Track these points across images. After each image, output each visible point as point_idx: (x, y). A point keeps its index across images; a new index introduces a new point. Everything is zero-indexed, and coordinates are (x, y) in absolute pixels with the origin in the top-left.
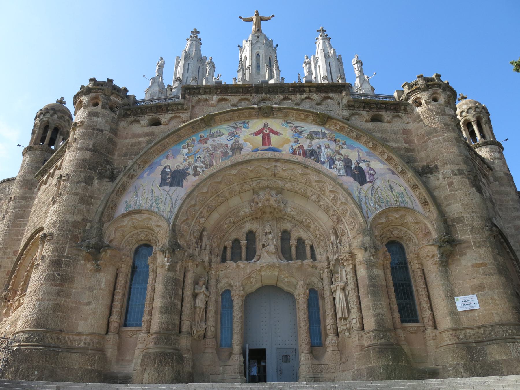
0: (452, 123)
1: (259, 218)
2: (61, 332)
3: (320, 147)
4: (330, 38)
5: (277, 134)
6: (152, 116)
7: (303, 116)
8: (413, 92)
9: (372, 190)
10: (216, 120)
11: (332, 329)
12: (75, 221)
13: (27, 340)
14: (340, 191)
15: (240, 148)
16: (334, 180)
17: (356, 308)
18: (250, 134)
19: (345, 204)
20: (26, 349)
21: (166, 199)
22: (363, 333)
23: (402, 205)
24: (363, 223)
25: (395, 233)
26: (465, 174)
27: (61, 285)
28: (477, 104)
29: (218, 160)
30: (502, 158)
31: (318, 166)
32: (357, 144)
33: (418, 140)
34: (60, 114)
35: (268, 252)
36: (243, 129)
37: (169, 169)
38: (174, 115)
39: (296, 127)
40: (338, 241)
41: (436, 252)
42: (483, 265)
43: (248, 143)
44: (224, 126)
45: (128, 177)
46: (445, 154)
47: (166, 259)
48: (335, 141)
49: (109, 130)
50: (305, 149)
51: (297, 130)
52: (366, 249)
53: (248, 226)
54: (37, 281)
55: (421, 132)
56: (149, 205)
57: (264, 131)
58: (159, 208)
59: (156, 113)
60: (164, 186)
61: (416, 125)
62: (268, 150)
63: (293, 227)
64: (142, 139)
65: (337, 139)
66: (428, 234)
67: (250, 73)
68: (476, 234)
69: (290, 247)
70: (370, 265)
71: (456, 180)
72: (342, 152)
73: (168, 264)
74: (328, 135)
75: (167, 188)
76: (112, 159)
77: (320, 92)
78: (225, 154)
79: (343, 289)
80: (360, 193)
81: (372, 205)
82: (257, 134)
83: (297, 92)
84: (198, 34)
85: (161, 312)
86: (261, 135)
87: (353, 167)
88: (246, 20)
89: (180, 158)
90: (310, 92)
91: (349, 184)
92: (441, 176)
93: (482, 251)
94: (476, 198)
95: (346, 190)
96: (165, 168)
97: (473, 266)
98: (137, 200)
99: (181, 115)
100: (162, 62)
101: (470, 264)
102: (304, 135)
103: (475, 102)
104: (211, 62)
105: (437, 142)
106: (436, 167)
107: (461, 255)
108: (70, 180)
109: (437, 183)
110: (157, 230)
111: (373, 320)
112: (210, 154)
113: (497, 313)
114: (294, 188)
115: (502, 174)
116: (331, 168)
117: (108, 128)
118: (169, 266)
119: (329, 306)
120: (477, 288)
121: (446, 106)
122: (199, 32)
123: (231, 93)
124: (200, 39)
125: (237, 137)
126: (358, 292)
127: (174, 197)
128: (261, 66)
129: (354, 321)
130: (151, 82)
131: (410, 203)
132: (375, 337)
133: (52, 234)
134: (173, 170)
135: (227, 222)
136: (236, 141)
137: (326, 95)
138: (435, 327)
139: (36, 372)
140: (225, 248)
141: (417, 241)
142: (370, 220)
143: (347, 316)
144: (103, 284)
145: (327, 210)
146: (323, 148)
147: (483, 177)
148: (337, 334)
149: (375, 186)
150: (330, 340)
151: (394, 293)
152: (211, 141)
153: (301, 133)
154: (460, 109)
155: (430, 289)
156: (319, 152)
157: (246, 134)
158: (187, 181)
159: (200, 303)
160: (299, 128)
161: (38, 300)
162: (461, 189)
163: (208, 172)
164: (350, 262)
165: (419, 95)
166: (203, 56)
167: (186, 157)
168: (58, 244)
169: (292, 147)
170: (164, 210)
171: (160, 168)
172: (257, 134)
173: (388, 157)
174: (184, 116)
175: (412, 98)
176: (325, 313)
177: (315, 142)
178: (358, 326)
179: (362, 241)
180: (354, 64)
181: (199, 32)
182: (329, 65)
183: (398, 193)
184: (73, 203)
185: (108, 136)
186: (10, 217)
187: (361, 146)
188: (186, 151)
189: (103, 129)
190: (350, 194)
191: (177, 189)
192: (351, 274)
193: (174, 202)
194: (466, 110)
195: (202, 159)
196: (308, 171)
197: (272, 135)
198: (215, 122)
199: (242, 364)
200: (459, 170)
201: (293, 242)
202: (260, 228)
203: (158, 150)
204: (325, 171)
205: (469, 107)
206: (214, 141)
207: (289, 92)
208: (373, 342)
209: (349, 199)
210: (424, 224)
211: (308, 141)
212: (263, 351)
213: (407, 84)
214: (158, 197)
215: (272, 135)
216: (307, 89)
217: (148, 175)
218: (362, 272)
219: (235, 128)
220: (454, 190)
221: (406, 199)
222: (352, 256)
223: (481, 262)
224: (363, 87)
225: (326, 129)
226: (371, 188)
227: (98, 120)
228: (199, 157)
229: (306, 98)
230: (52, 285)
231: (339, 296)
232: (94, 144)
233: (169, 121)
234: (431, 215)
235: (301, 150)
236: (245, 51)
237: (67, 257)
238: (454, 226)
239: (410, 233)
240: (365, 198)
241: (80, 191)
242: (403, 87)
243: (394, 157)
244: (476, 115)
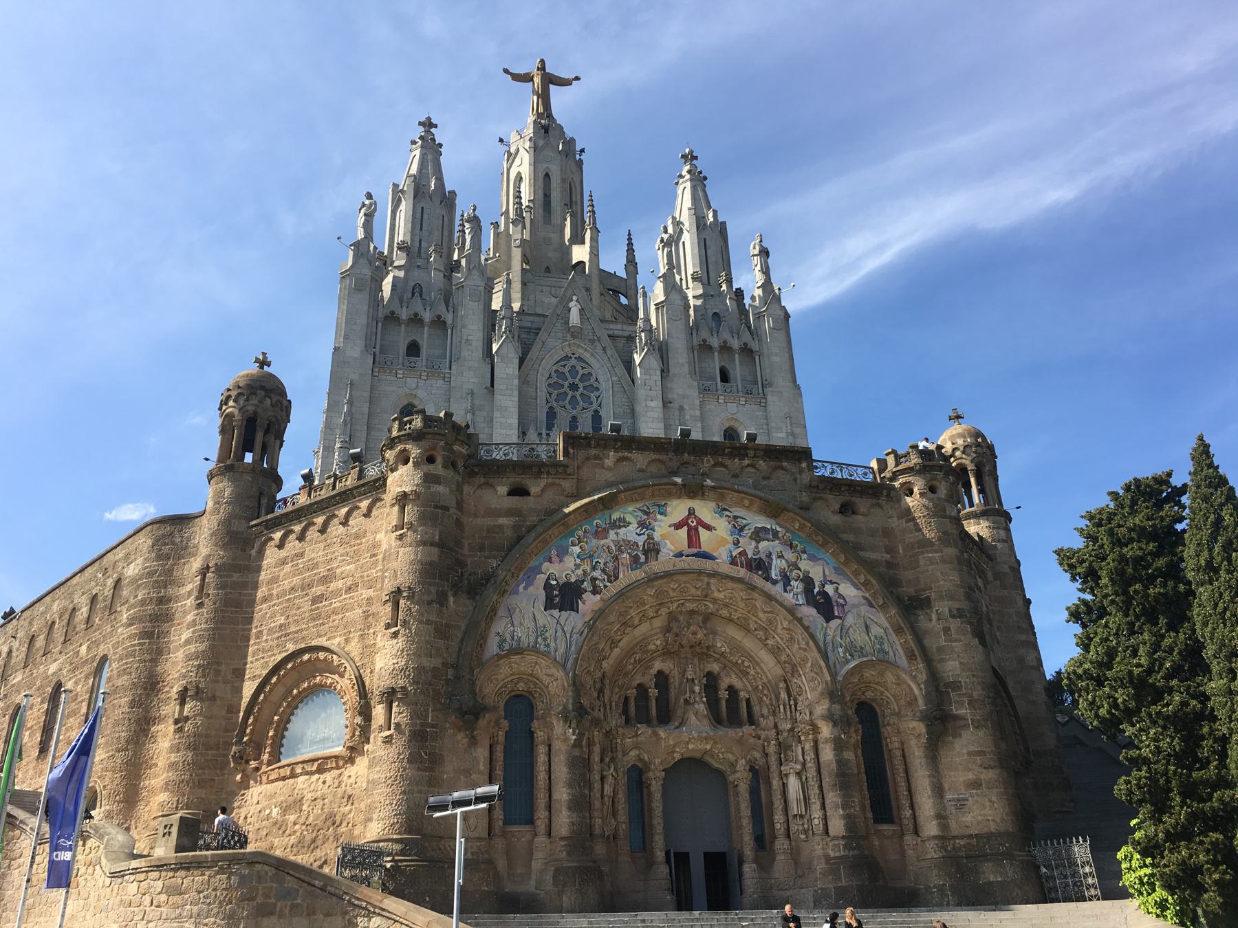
0: (954, 531)
1: (673, 653)
2: (442, 838)
3: (769, 555)
4: (705, 178)
5: (708, 528)
6: (514, 479)
7: (747, 503)
8: (903, 472)
10: (619, 499)
11: (783, 829)
12: (434, 668)
13: (402, 853)
14: (800, 630)
15: (658, 551)
16: (791, 611)
17: (818, 803)
18: (670, 526)
19: (805, 650)
20: (407, 866)
21: (556, 632)
22: (828, 840)
23: (881, 656)
24: (829, 683)
25: (869, 694)
26: (966, 616)
27: (432, 769)
28: (979, 440)
29: (626, 568)
30: (1008, 540)
31: (768, 586)
32: (821, 554)
33: (903, 549)
34: (275, 398)
35: (696, 714)
36: (659, 517)
37: (556, 580)
38: (550, 480)
39: (735, 517)
40: (792, 702)
41: (924, 730)
42: (979, 753)
44: (631, 509)
45: (499, 593)
46: (942, 582)
47: (571, 730)
48: (791, 546)
49: (455, 506)
51: (737, 522)
52: (835, 724)
53: (658, 665)
54: (395, 762)
55: (910, 538)
56: (532, 640)
57: (690, 522)
58: (547, 646)
59: (521, 474)
60: (551, 609)
61: (903, 523)
62: (697, 555)
63: (724, 668)
64: (503, 521)
65: (795, 543)
66: (912, 702)
67: (531, 219)
68: (975, 709)
69: (718, 700)
70: (839, 746)
71: (955, 624)
73: (574, 737)
74: (780, 535)
75: (556, 612)
76: (462, 555)
77: (769, 457)
78: (635, 559)
79: (799, 774)
80: (825, 635)
81: (842, 654)
82: (678, 526)
83: (735, 455)
84: (433, 130)
85: (570, 808)
86: (685, 528)
87: (816, 590)
88: (517, 77)
89: (570, 562)
90: (755, 456)
91: (811, 619)
92: (934, 616)
93: (981, 734)
94: (978, 655)
95: (806, 629)
96: (548, 578)
97: (969, 754)
98: (514, 631)
99: (563, 483)
100: (371, 205)
101: (965, 751)
102: (748, 532)
103: (977, 433)
104: (475, 216)
105: (931, 561)
106: (928, 600)
107: (954, 737)
108: (416, 597)
109: (929, 625)
110: (546, 680)
111: (842, 822)
112: (613, 557)
113: (993, 820)
114: (731, 615)
115: (1006, 569)
116: (785, 591)
117: (454, 504)
118: (575, 740)
119: (777, 797)
120: (971, 784)
121: (947, 501)
122: (436, 126)
123: (638, 449)
124: (440, 145)
125: (651, 529)
126: (821, 782)
127: (568, 629)
128: (552, 205)
129: (816, 821)
130: (351, 253)
131: (891, 653)
132: (845, 847)
133: (404, 688)
134: (561, 582)
135: (632, 661)
136: (650, 537)
137: (778, 463)
138: (916, 832)
139: (428, 899)
140: (627, 699)
141: (896, 708)
142: (840, 678)
143: (804, 813)
144: (481, 764)
145: (775, 651)
146: (774, 557)
147: (980, 577)
148: (788, 836)
149: (846, 624)
150: (781, 844)
151: (866, 784)
152: (612, 533)
153: (742, 529)
154: (953, 444)
155: (913, 781)
156: (768, 563)
157: (663, 524)
158: (584, 603)
159: (608, 790)
160: (739, 520)
161: (403, 793)
162: (960, 640)
163: (613, 588)
164: (811, 737)
165: (911, 478)
166: (447, 189)
167: (578, 561)
168: (416, 704)
169: (731, 552)
170: (556, 650)
171: (541, 579)
172: (678, 526)
173: (866, 580)
174: (568, 485)
175: (901, 480)
176: (771, 803)
177: (763, 545)
178: (821, 829)
179: (829, 710)
180: (754, 255)
181: (436, 126)
182: (703, 245)
183: (876, 636)
184: (427, 638)
185: (455, 517)
186: (214, 604)
187: (827, 556)
188: (577, 549)
189: (448, 505)
190: (812, 637)
191: (570, 615)
192: (810, 757)
193: (568, 636)
194: (962, 449)
195: (602, 564)
196: (756, 595)
197: (701, 529)
198: (617, 503)
199: (669, 877)
200: (958, 609)
201: (723, 694)
202: (676, 669)
203: (537, 548)
204: (778, 597)
205: (966, 444)
206: (617, 534)
207: (724, 454)
208: (842, 853)
209: (811, 643)
210: (909, 686)
211: (754, 543)
212: (686, 855)
213: (894, 452)
214: (545, 627)
215: (701, 529)
216: (751, 453)
217: (525, 588)
218: (827, 754)
219: (647, 513)
220: (951, 641)
221: (886, 647)
222: (815, 729)
223: (979, 749)
224: (770, 311)
225: (777, 524)
227: (440, 489)
228: (598, 562)
229: (748, 465)
230: (419, 769)
231: (793, 783)
232: (440, 535)
233: (542, 490)
234: (919, 676)
236: (517, 161)
237: (433, 726)
238: (948, 693)
239: (889, 695)
240: (833, 642)
241: (433, 618)
242: (888, 454)
243: (874, 582)
244: (976, 460)
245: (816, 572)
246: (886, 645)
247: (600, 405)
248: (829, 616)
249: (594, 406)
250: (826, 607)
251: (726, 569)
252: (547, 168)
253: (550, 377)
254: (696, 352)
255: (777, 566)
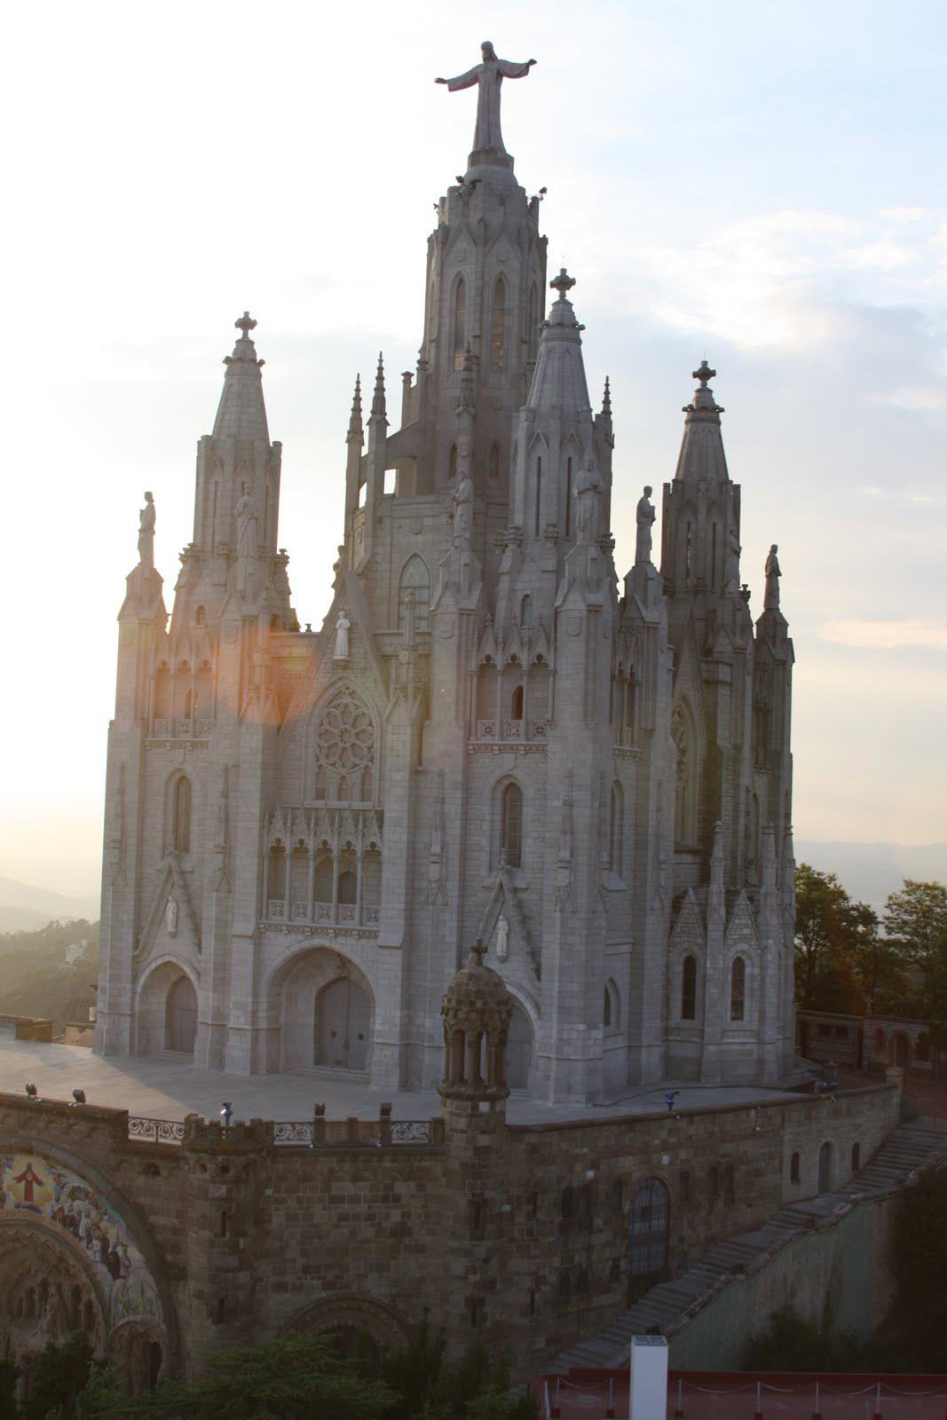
3: (80, 1214)
5: (40, 1183)
9: (124, 1288)
16: (88, 1268)
32: (117, 1216)
36: (7, 1170)
39: (60, 1175)
43: (11, 1193)
48: (97, 1207)
50: (66, 1213)
53: (41, 1276)
62: (30, 1207)
72: (103, 1225)
74: (90, 1195)
80: (111, 1291)
81: (121, 1310)
86: (24, 1182)
102: (67, 1190)
146: (83, 1215)
153: (62, 1188)
172: (20, 1179)
177: (77, 1203)
211: (70, 1200)
215: (35, 1185)
226: (121, 1288)
235: (61, 1214)
245: (114, 1232)
246: (154, 1306)
247: (372, 760)
248: (116, 1276)
249: (364, 763)
250: (115, 1265)
251: (47, 1222)
252: (459, 272)
253: (322, 724)
254: (475, 679)
255: (84, 1222)
